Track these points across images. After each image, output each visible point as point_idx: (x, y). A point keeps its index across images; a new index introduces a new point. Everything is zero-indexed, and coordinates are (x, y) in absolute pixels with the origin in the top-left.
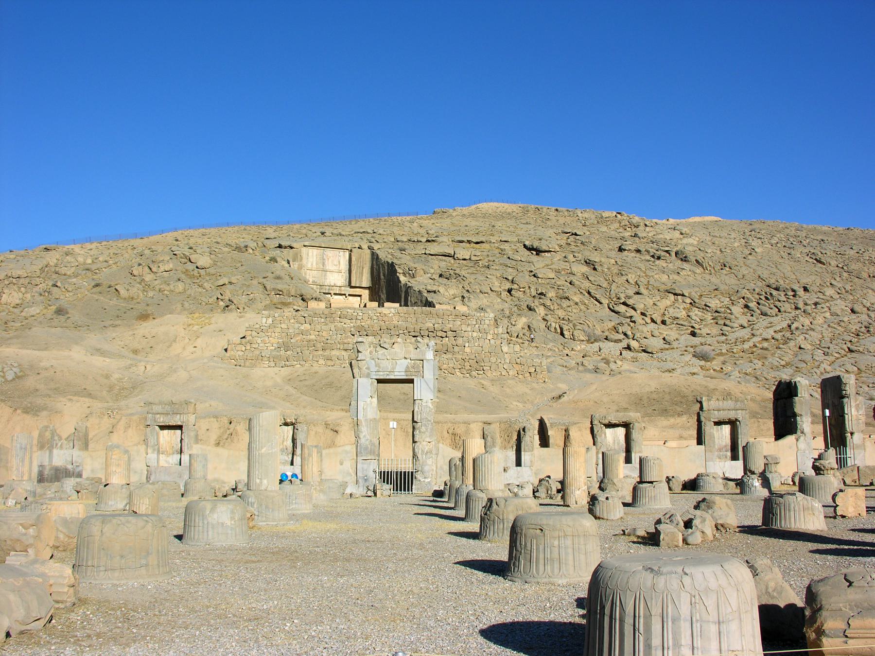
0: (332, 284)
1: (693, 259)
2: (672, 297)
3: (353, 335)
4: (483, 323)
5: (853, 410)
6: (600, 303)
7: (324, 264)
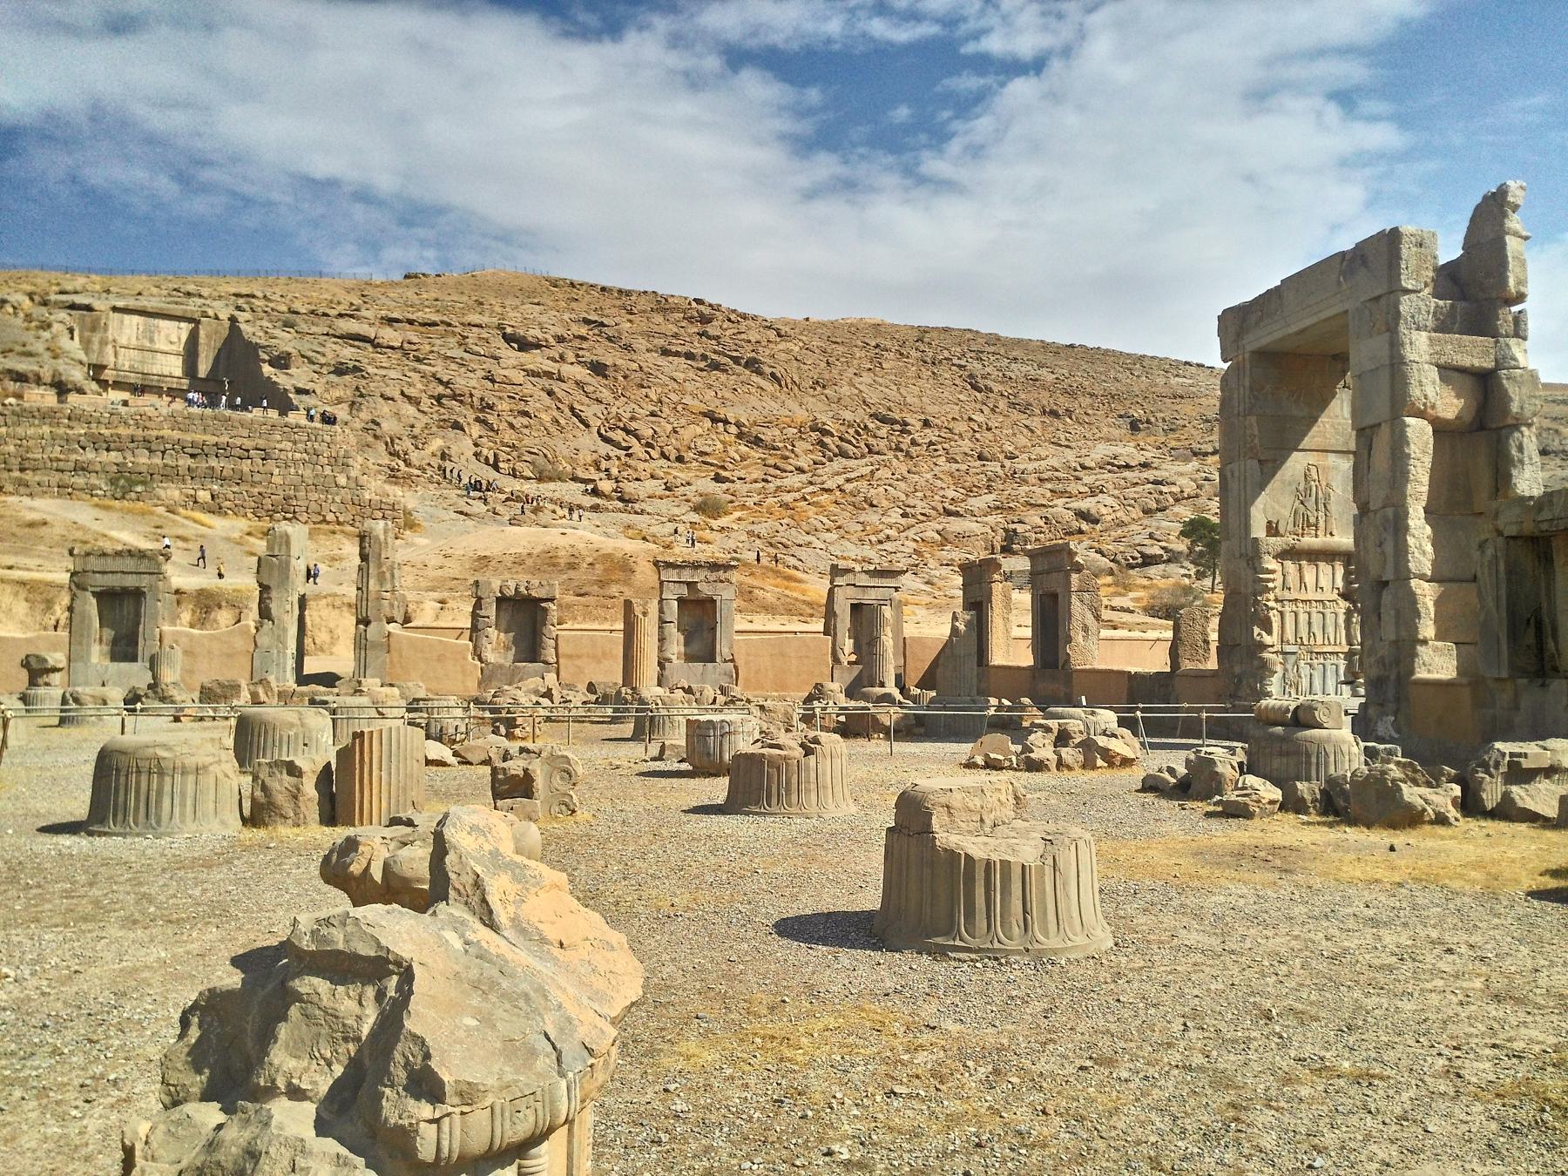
1: (768, 370)
2: (708, 423)
3: (84, 448)
4: (319, 439)
5: (372, 582)
6: (587, 426)
7: (152, 340)
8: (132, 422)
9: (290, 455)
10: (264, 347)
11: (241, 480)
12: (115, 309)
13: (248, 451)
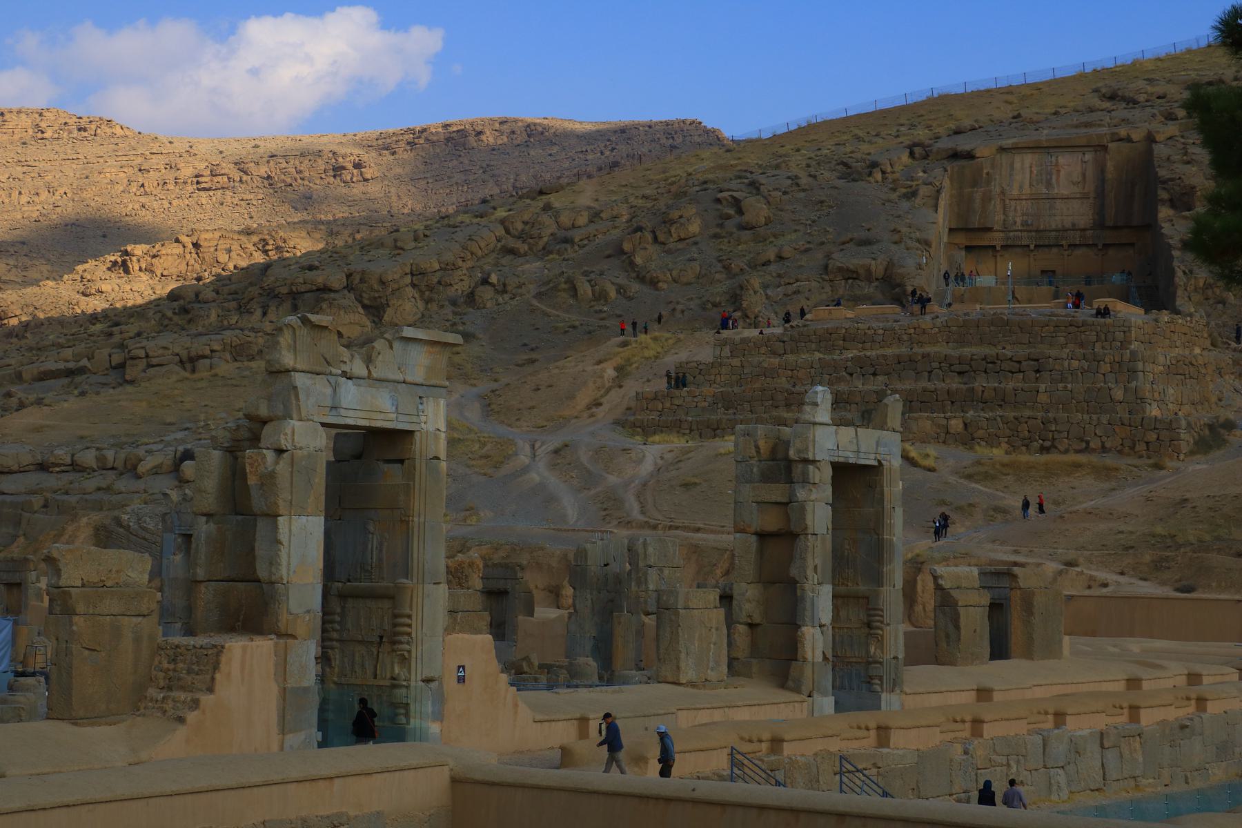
0: (1068, 225)
3: (851, 375)
4: (1110, 337)
5: (633, 584)
7: (1049, 184)
8: (905, 337)
9: (1066, 363)
10: (1164, 182)
11: (1002, 400)
12: (1002, 150)
13: (1019, 362)
